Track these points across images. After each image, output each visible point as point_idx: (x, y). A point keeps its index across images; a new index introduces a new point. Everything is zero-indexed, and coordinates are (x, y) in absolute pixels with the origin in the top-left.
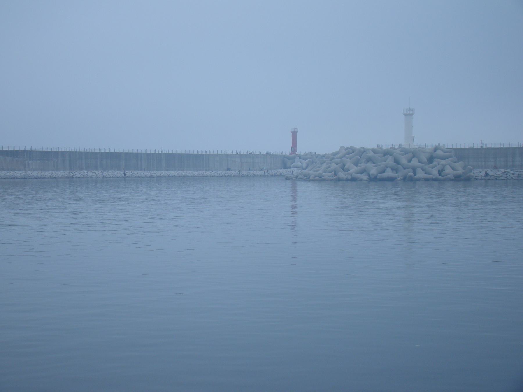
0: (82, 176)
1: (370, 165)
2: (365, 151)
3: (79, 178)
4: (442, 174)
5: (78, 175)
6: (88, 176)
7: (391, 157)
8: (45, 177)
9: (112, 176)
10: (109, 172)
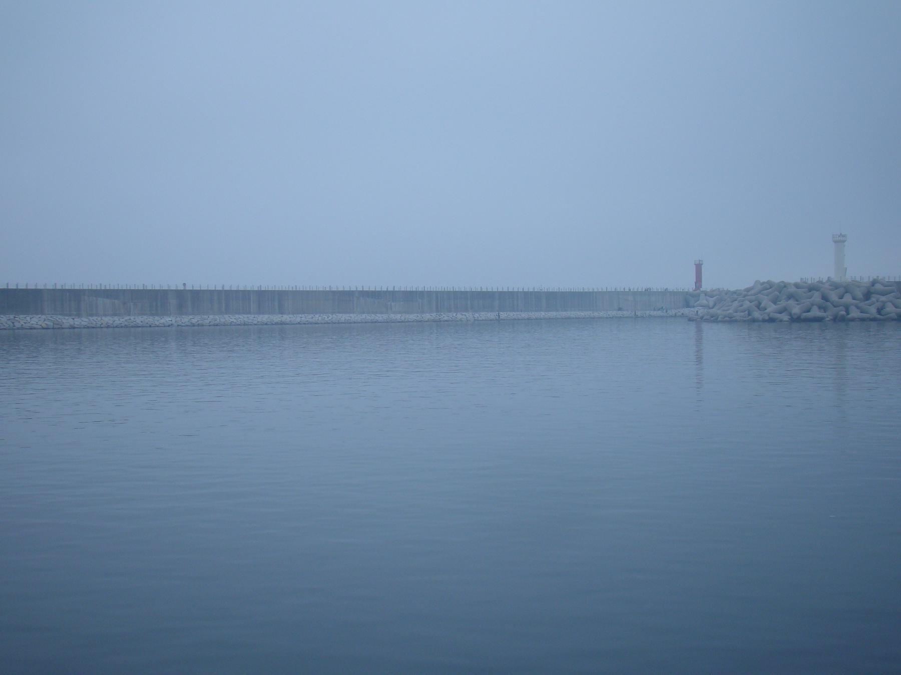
0: (451, 319)
1: (791, 302)
2: (785, 287)
3: (447, 321)
4: (883, 312)
5: (446, 318)
7: (818, 292)
8: (409, 320)
9: (484, 318)
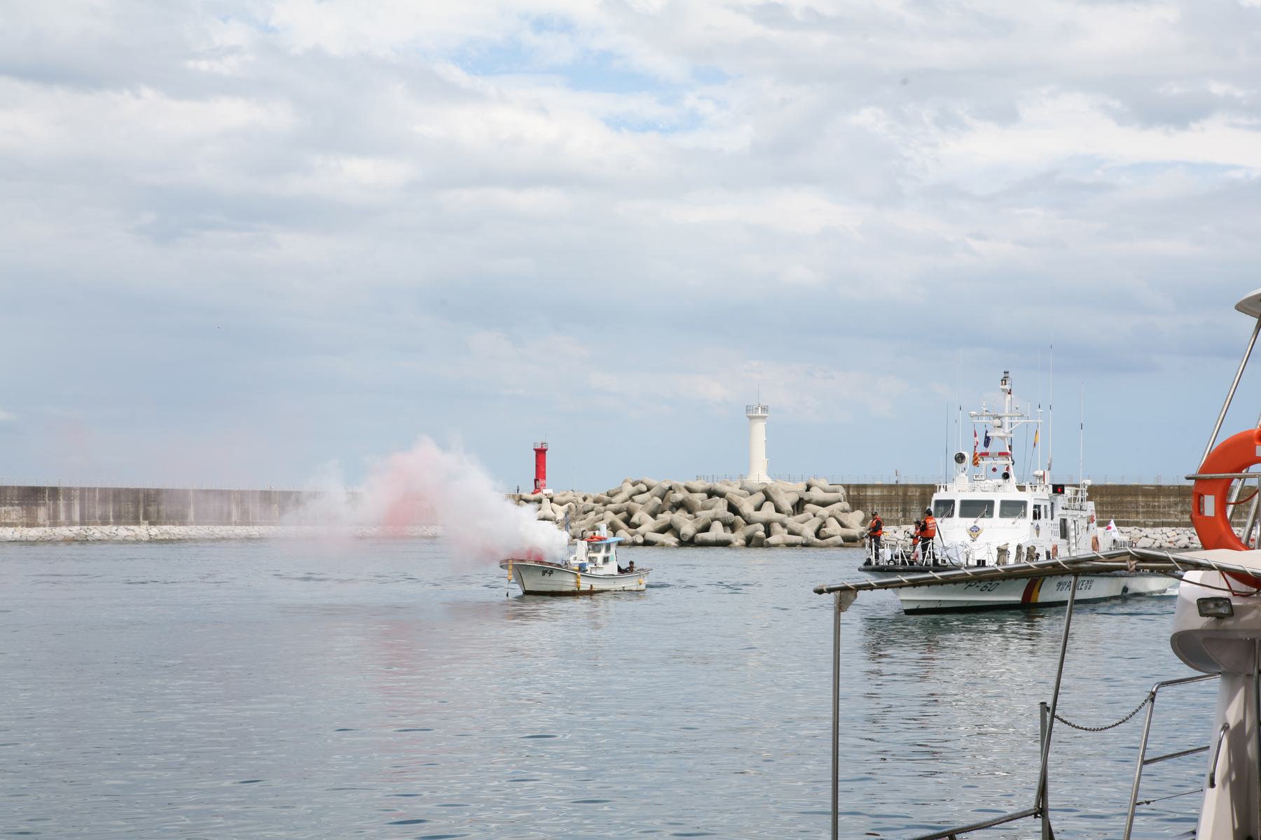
0: (106, 538)
5: (98, 535)
6: (118, 538)
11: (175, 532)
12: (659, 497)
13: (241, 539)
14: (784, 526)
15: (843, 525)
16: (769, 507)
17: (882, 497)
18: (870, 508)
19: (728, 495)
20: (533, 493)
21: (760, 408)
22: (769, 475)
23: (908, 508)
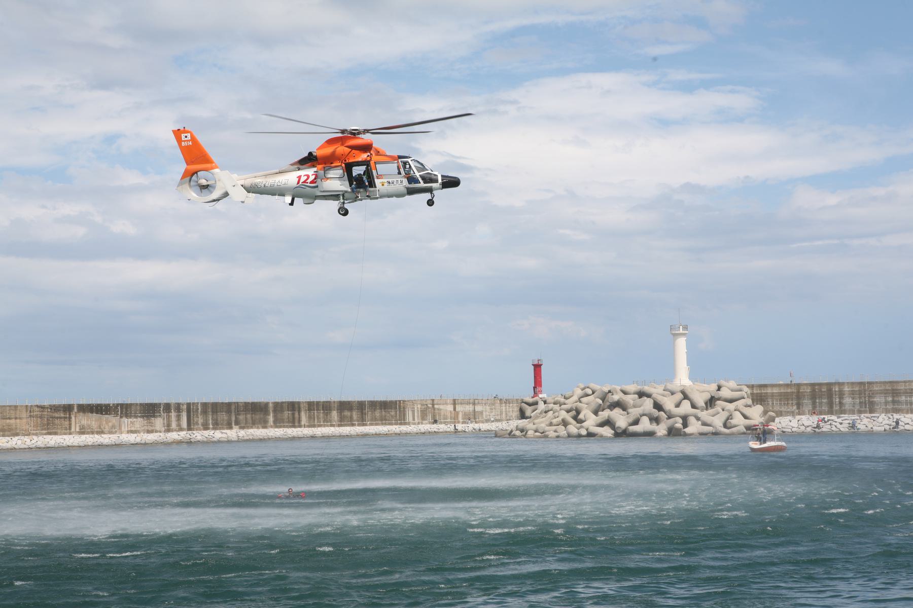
0: (205, 440)
5: (199, 438)
10: (248, 432)
11: (258, 434)
12: (601, 399)
13: (307, 437)
14: (698, 419)
15: (745, 417)
16: (686, 405)
17: (780, 394)
18: (770, 403)
19: (654, 396)
20: (533, 397)
21: (681, 327)
22: (690, 379)
23: (801, 401)
